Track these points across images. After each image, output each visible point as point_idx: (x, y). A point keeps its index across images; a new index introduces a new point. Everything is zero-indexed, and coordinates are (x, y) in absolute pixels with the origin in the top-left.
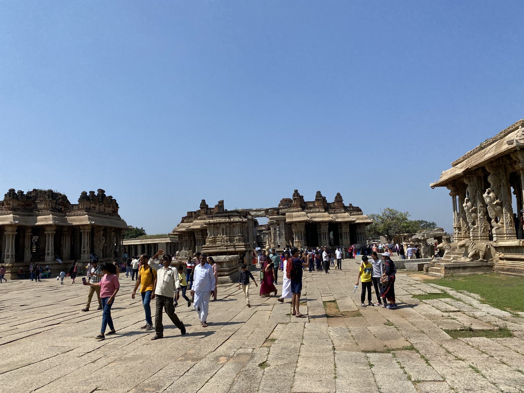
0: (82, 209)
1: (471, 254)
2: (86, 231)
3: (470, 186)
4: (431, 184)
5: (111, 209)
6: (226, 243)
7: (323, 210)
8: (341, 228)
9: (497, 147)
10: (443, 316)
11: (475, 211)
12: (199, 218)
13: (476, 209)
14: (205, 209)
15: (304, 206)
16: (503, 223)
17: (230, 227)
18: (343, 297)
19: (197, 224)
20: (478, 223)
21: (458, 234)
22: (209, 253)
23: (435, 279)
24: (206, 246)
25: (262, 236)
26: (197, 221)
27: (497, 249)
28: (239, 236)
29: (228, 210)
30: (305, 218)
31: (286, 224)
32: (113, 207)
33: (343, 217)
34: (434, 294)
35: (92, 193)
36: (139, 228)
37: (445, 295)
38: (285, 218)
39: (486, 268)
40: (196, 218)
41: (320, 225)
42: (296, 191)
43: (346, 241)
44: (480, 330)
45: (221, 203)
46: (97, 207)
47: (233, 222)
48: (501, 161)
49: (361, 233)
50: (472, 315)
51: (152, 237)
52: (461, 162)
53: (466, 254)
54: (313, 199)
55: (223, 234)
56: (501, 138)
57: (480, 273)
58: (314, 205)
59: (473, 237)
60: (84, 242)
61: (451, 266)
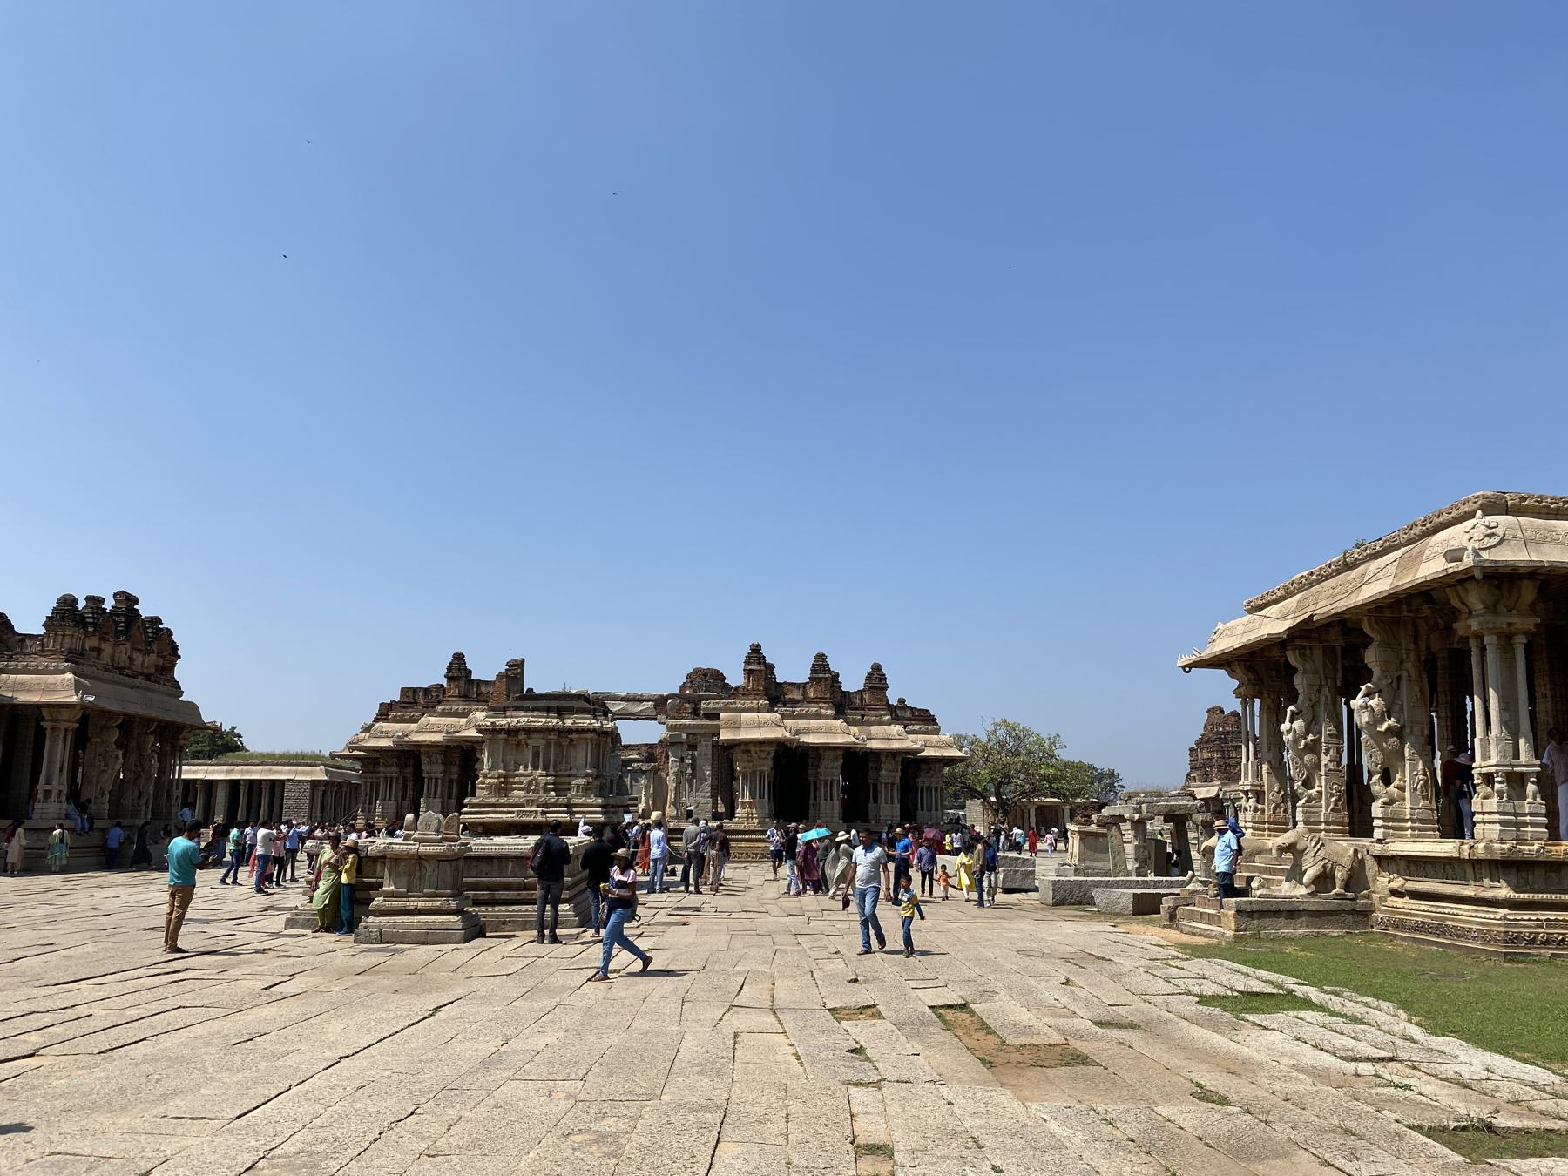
0: (54, 652)
1: (1310, 873)
2: (63, 726)
3: (1305, 672)
4: (1186, 660)
5: (152, 659)
6: (542, 797)
8: (878, 769)
9: (1403, 566)
10: (1357, 1075)
11: (1313, 748)
12: (439, 709)
13: (1317, 742)
14: (462, 683)
15: (773, 693)
16: (1402, 789)
17: (559, 745)
18: (987, 994)
19: (430, 730)
20: (1321, 785)
21: (1255, 810)
22: (483, 824)
23: (1209, 946)
24: (475, 801)
25: (628, 780)
26: (433, 719)
27: (1384, 864)
28: (586, 776)
29: (538, 691)
31: (716, 745)
32: (160, 654)
33: (887, 737)
34: (1257, 994)
35: (95, 601)
36: (226, 728)
37: (1289, 1001)
38: (718, 727)
39: (1350, 918)
40: (429, 708)
41: (820, 758)
42: (756, 649)
43: (888, 808)
44: (1517, 1130)
46: (107, 648)
47: (570, 731)
48: (1404, 607)
49: (929, 788)
50: (1451, 1075)
52: (1276, 602)
53: (1296, 874)
54: (803, 676)
55: (535, 767)
56: (1411, 542)
57: (1335, 933)
58: (805, 694)
59: (1306, 822)
60: (50, 762)
61: (1255, 908)
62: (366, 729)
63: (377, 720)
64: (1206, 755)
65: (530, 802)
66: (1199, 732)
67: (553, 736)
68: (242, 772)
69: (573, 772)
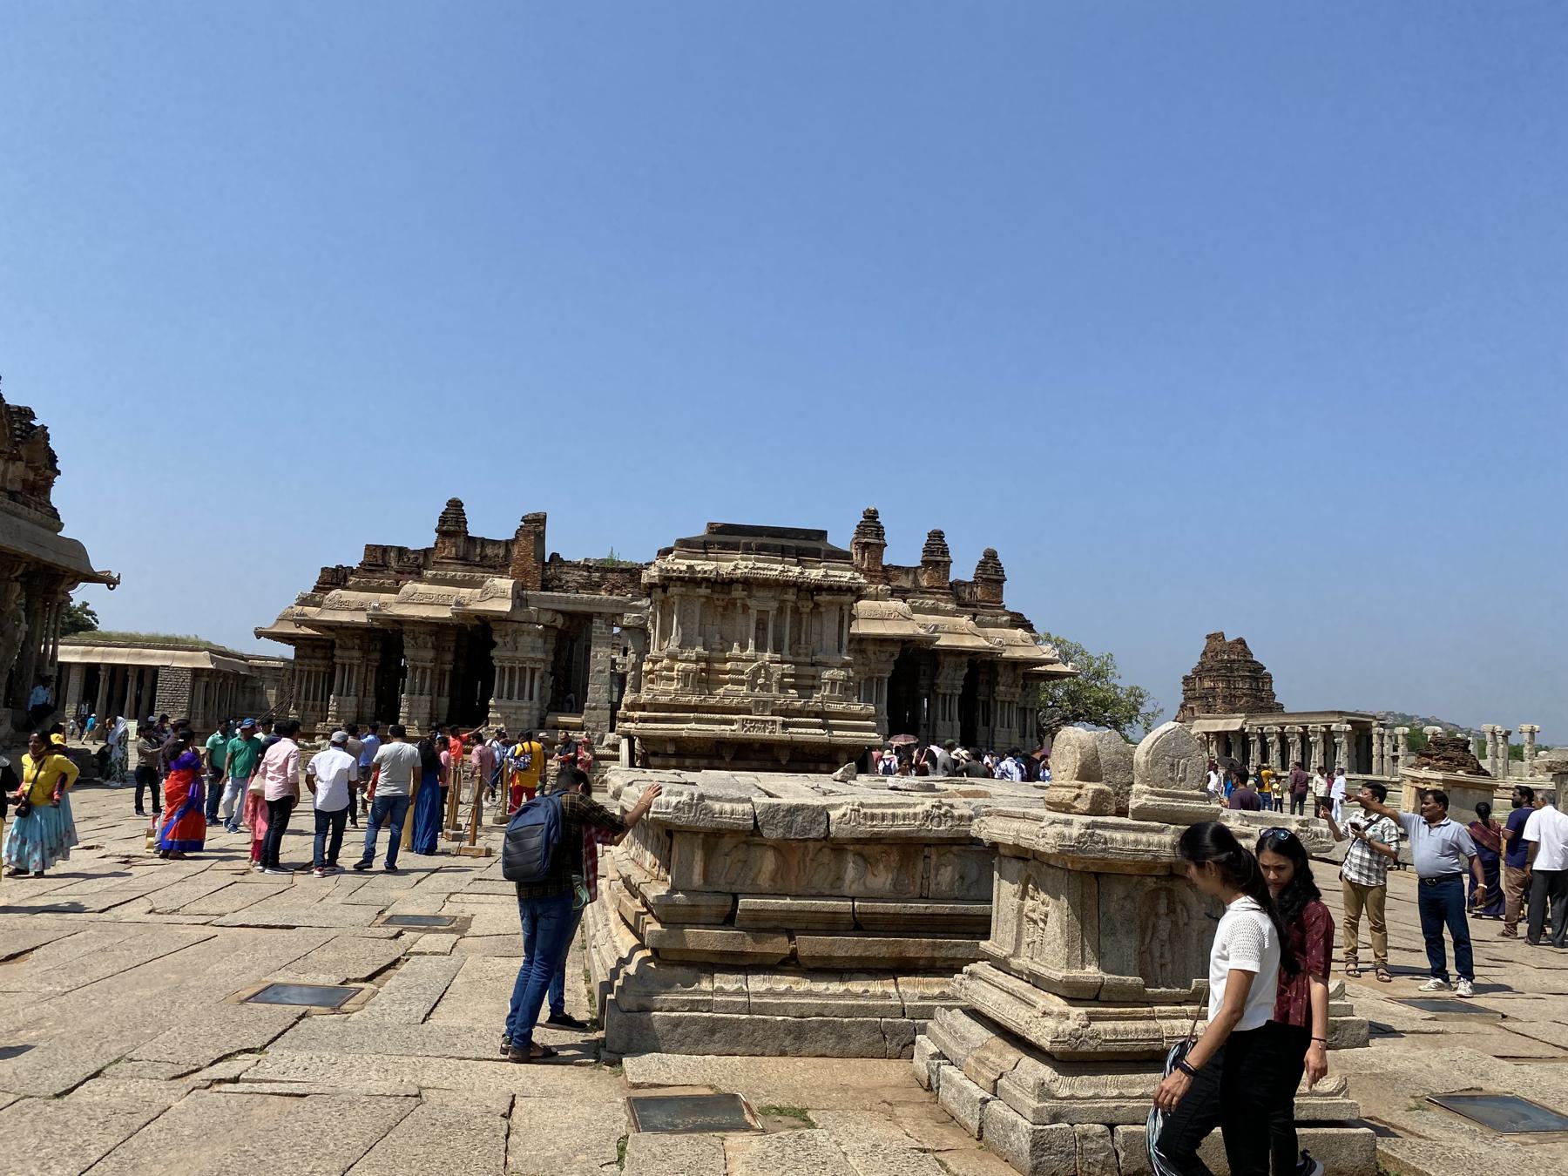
5: (17, 470)
7: (950, 606)
8: (992, 683)
12: (429, 573)
14: (461, 541)
17: (796, 610)
22: (677, 741)
26: (422, 587)
30: (905, 629)
32: (30, 464)
40: (416, 573)
45: (535, 526)
47: (818, 588)
51: (131, 641)
54: (914, 559)
55: (760, 647)
58: (916, 581)
62: (304, 601)
63: (316, 589)
64: (1207, 684)
65: (762, 705)
66: (1194, 661)
67: (791, 596)
68: (103, 654)
69: (820, 657)
